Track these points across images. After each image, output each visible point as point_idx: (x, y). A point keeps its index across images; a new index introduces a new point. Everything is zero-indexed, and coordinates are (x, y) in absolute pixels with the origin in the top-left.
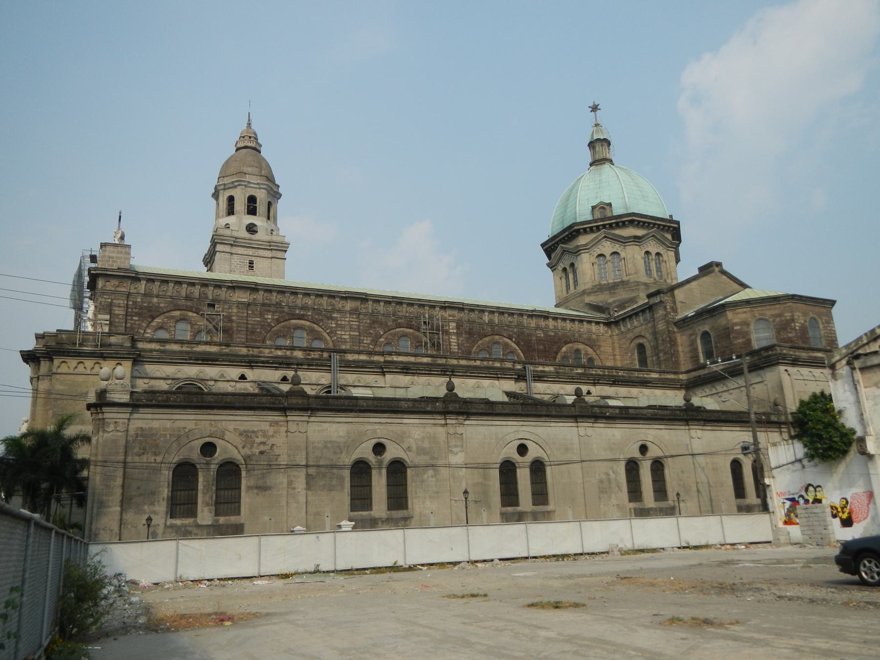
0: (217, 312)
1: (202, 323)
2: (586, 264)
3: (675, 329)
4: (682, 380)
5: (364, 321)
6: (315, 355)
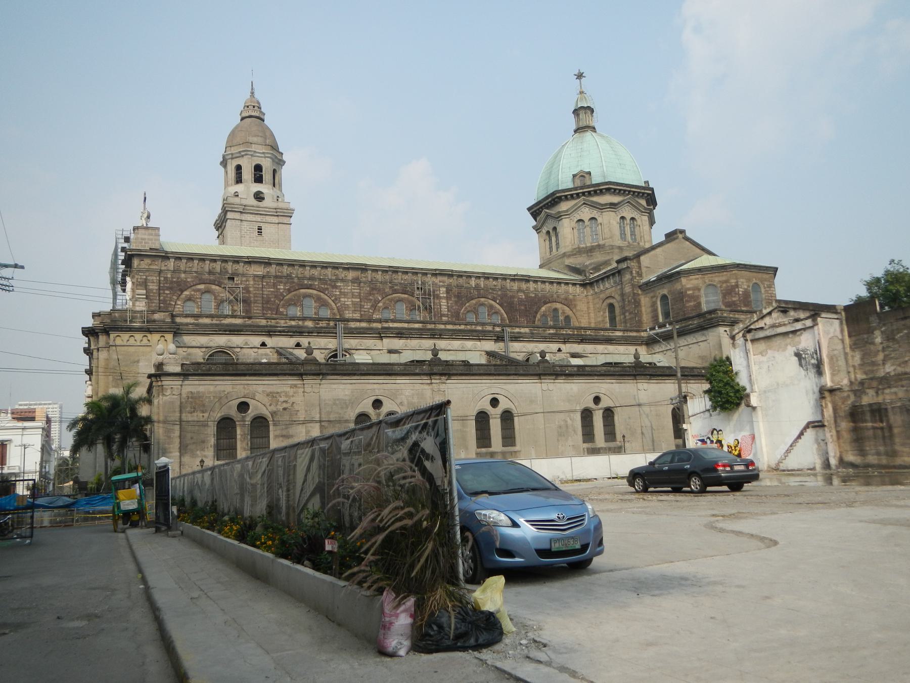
0: (236, 284)
1: (224, 295)
2: (566, 228)
3: (640, 292)
4: (643, 337)
5: (365, 288)
6: (323, 324)
